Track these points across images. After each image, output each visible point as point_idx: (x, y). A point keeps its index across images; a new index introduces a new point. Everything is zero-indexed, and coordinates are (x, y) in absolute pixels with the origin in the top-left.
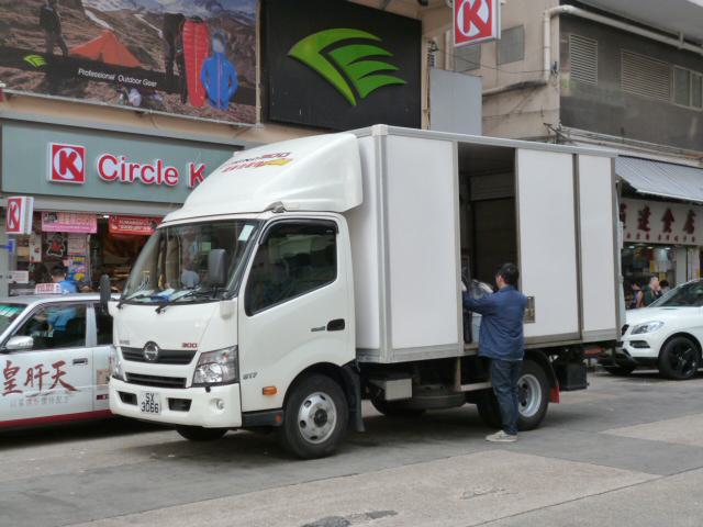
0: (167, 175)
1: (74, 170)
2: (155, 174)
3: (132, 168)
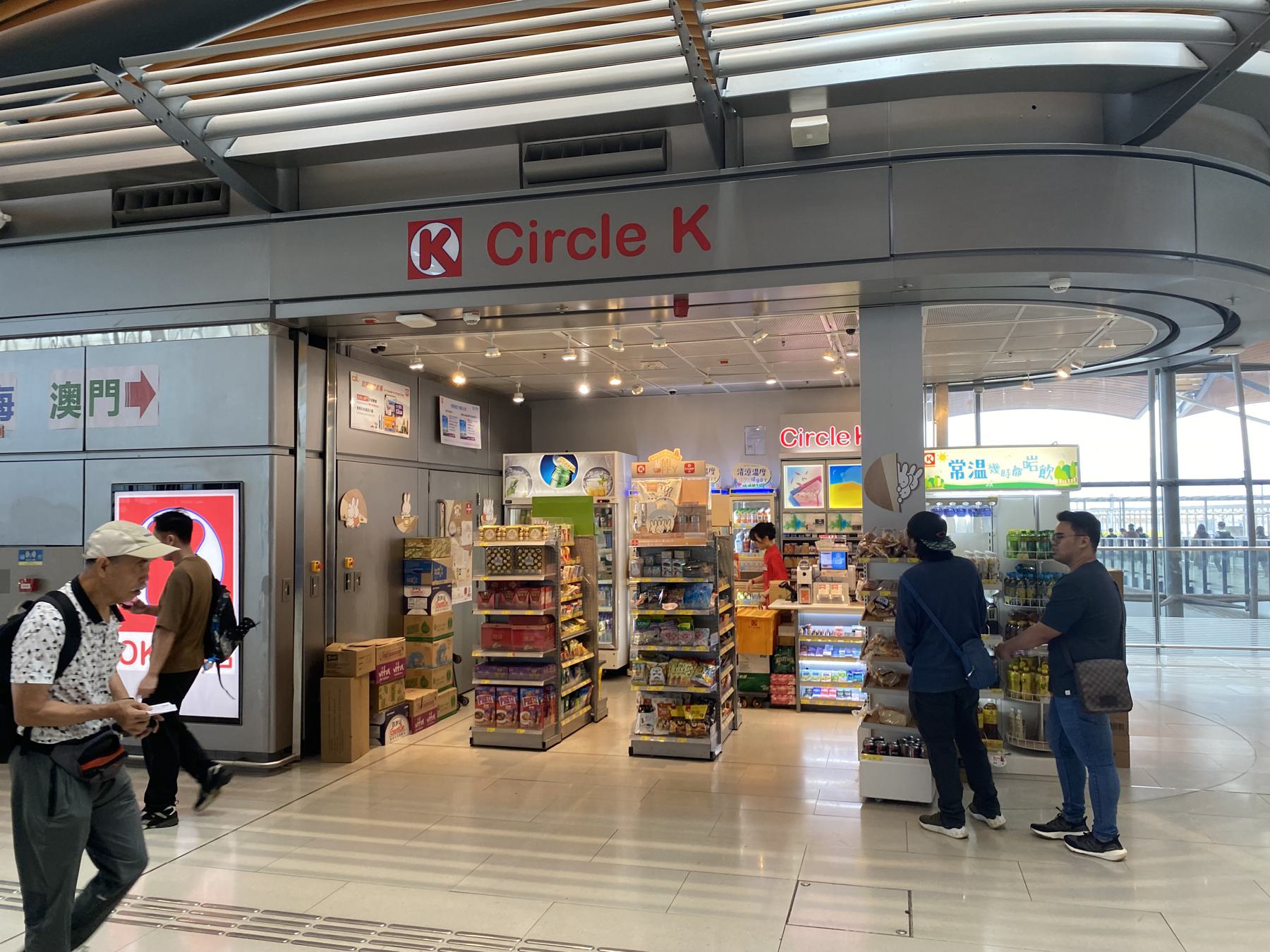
0: (621, 240)
1: (444, 259)
2: (597, 242)
3: (550, 237)
